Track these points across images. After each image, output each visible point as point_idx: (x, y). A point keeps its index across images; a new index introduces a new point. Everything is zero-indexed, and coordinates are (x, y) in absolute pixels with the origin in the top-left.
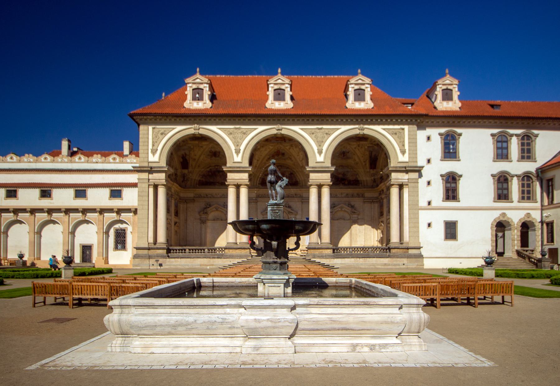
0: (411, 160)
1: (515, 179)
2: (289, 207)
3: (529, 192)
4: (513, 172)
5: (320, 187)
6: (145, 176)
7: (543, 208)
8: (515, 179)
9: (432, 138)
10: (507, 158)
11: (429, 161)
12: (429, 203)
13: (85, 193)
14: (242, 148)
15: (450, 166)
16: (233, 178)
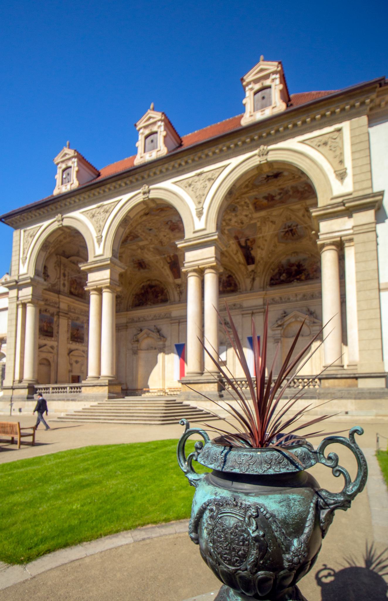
0: (357, 188)
16: (94, 280)
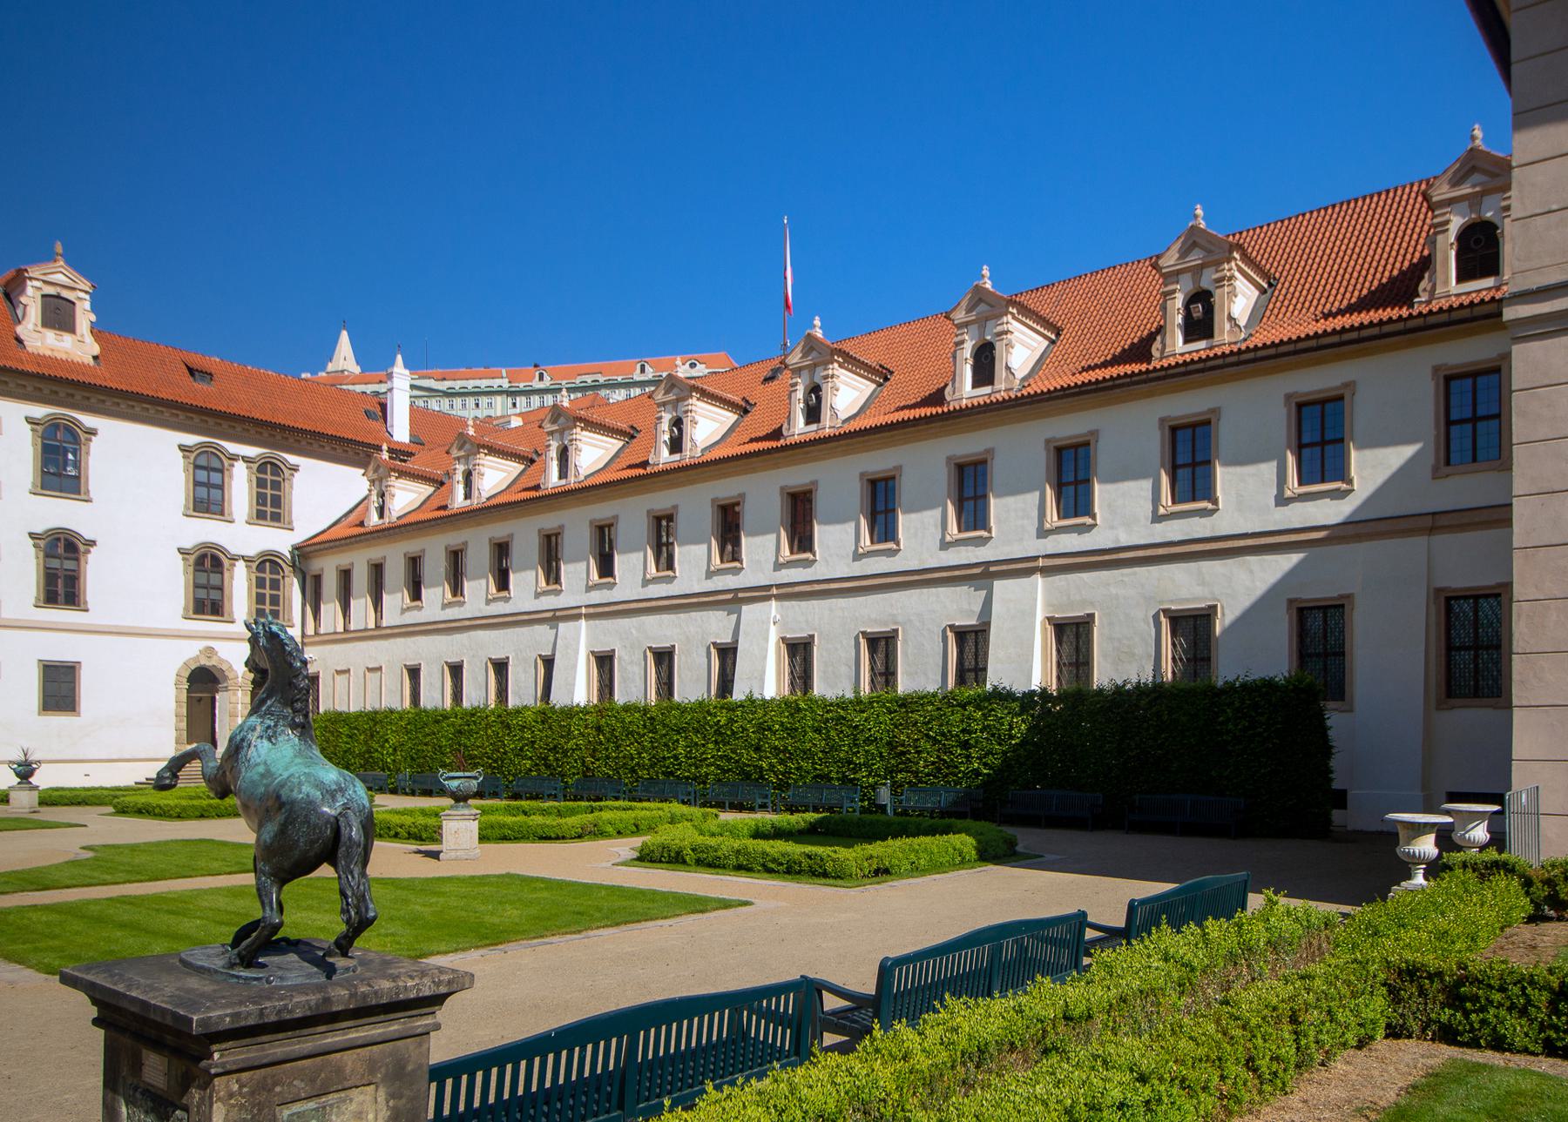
1: (241, 565)
3: (275, 600)
7: (305, 640)
8: (241, 565)
10: (222, 514)
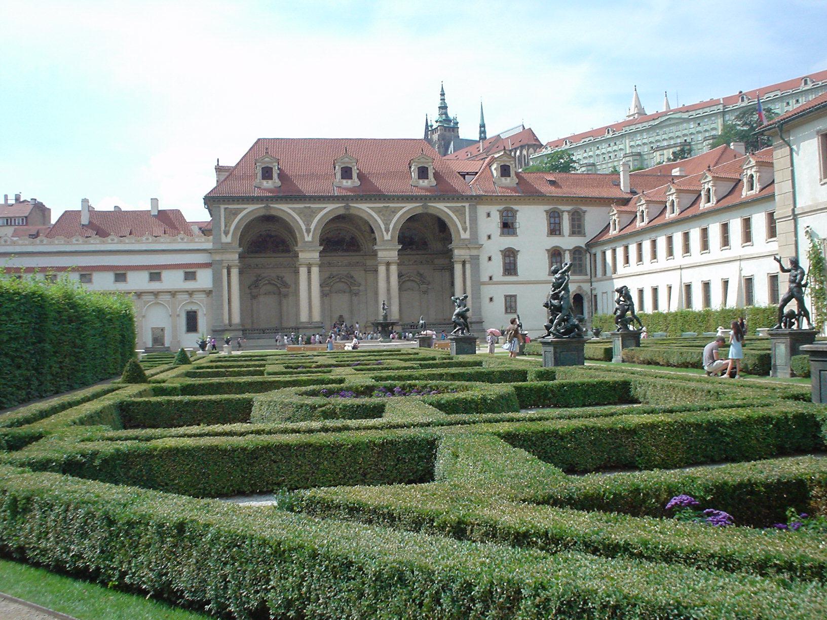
1: (567, 252)
2: (352, 277)
3: (580, 265)
4: (564, 247)
5: (388, 264)
6: (218, 257)
8: (567, 252)
9: (492, 215)
11: (489, 237)
12: (491, 278)
13: (160, 276)
14: (313, 227)
15: (509, 242)
